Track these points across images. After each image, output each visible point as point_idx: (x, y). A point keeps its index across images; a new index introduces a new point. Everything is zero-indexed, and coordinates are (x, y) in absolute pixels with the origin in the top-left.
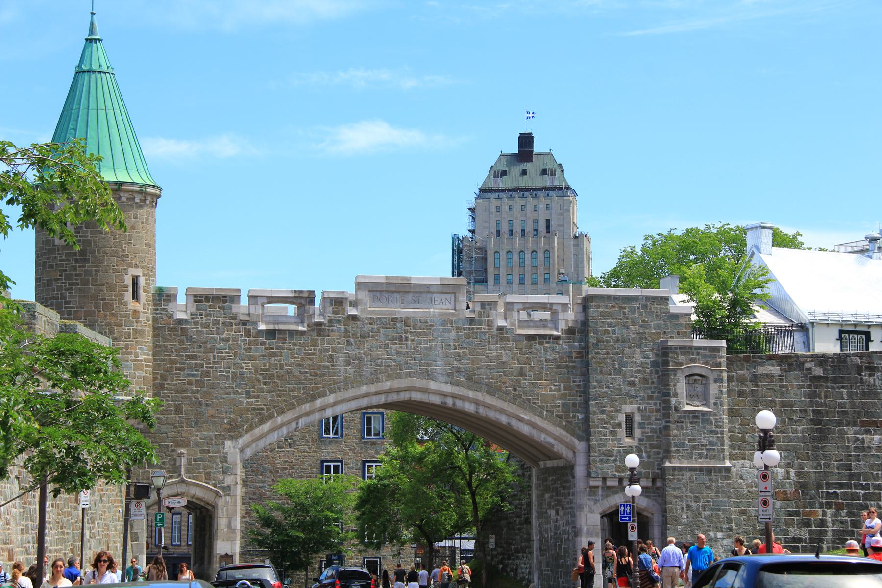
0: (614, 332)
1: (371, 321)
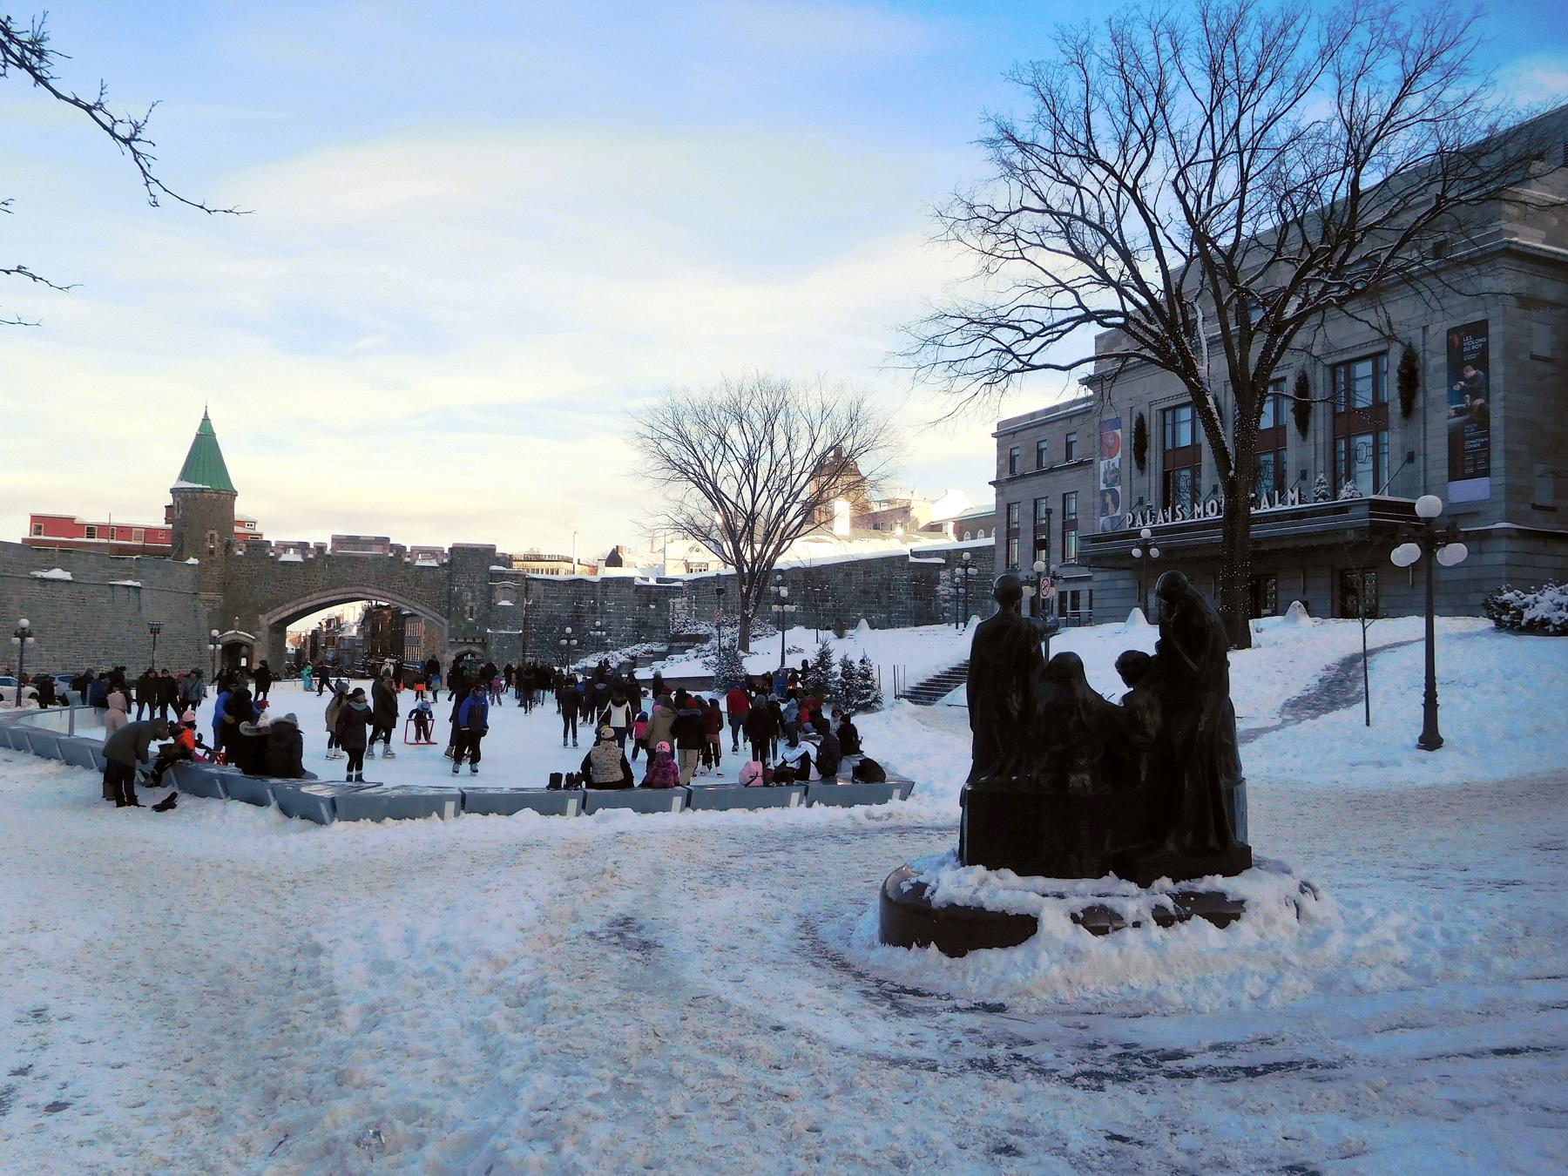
1: (337, 558)
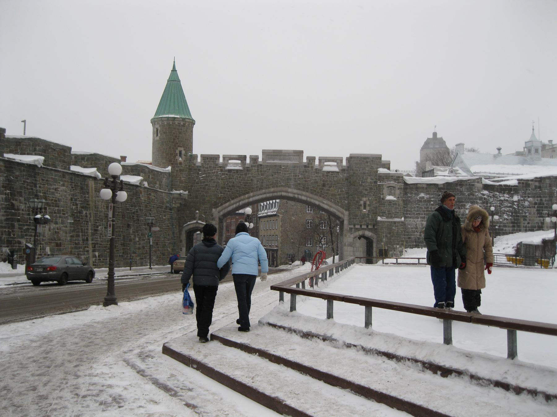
0: (360, 170)
